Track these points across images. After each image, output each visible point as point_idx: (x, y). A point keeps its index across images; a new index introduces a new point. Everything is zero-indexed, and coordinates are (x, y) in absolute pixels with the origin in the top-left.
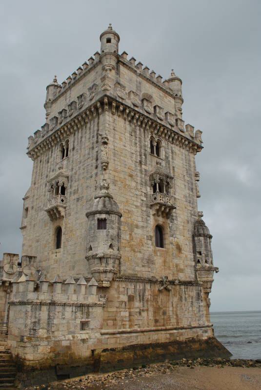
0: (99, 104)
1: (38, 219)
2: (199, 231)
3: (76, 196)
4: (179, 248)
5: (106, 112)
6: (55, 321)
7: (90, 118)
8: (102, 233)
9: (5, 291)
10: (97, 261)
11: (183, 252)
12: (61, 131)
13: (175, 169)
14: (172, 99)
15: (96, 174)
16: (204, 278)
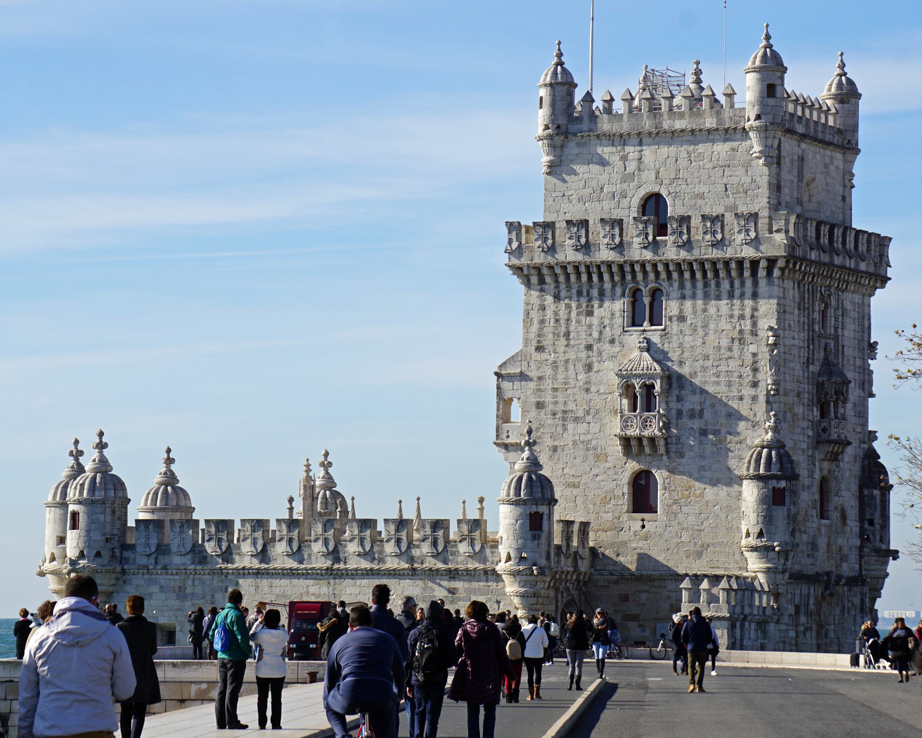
0: (763, 264)
1: (568, 438)
2: (874, 476)
3: (696, 424)
4: (844, 517)
5: (776, 281)
6: (745, 642)
7: (734, 274)
8: (780, 513)
9: (556, 589)
10: (772, 555)
11: (849, 522)
12: (643, 266)
13: (846, 349)
14: (839, 156)
15: (754, 398)
16: (874, 570)
